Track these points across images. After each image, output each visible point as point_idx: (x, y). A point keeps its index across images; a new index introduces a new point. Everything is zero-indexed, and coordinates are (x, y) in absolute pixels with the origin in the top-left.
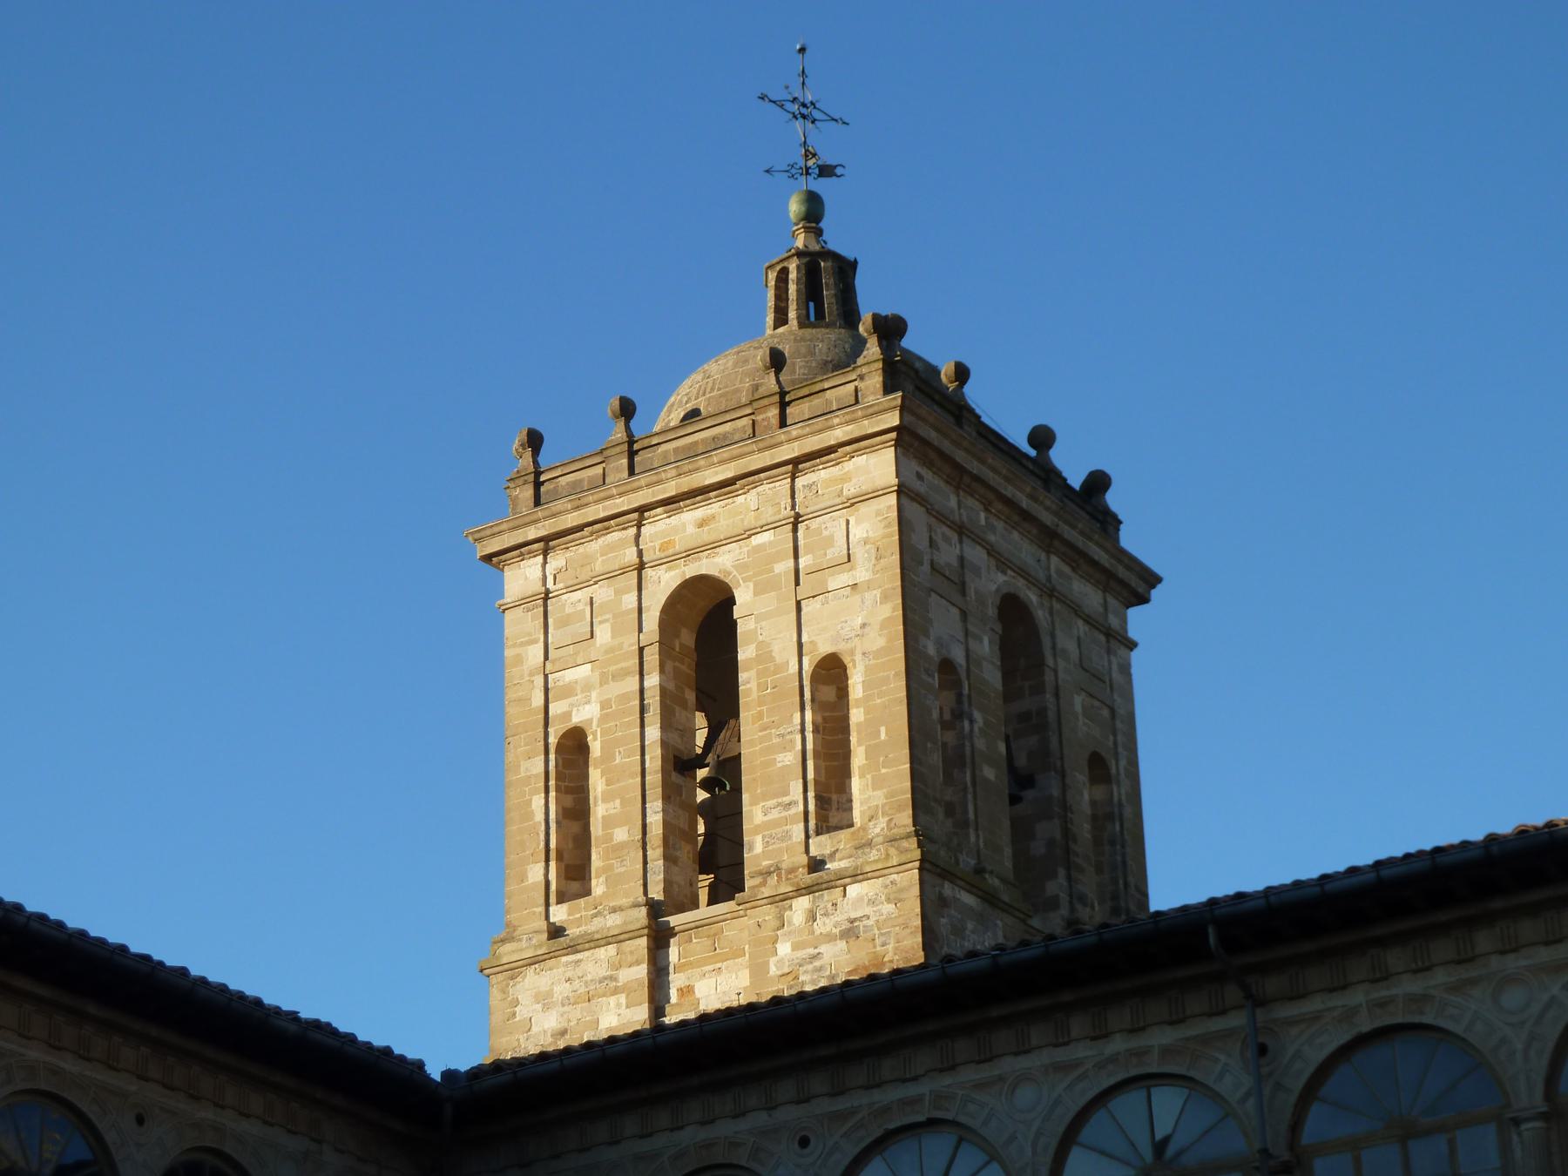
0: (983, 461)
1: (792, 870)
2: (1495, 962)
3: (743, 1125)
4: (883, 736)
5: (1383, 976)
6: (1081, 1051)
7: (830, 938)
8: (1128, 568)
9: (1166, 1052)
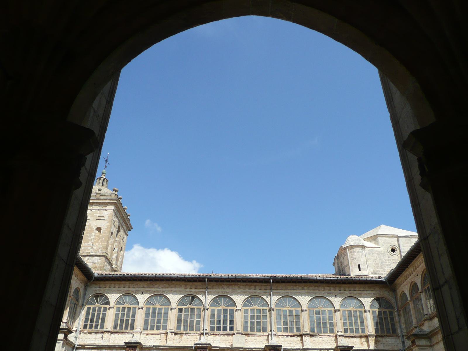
0: (122, 209)
1: (87, 252)
3: (134, 289)
4: (104, 239)
6: (183, 289)
7: (90, 262)
8: (130, 226)
9: (194, 292)
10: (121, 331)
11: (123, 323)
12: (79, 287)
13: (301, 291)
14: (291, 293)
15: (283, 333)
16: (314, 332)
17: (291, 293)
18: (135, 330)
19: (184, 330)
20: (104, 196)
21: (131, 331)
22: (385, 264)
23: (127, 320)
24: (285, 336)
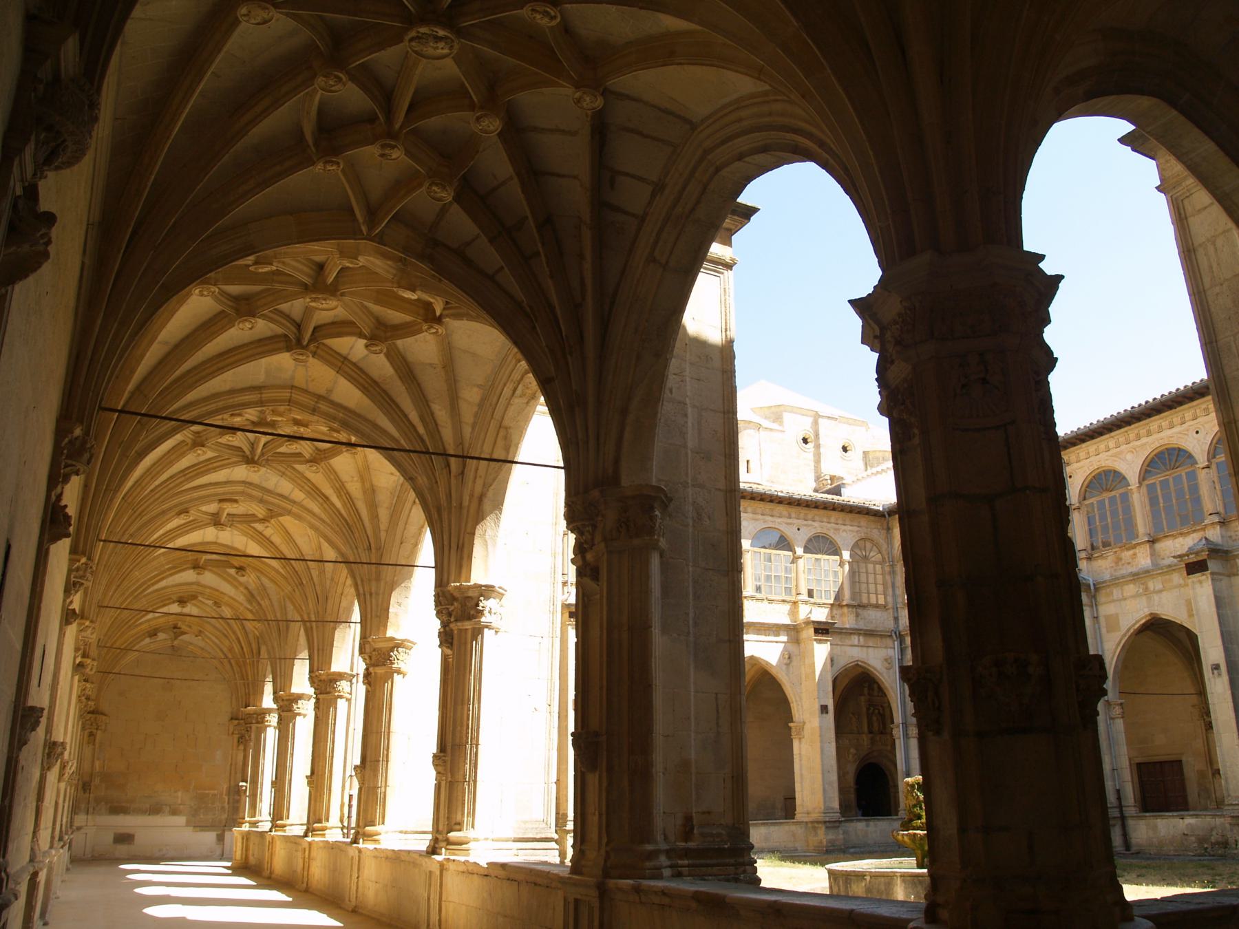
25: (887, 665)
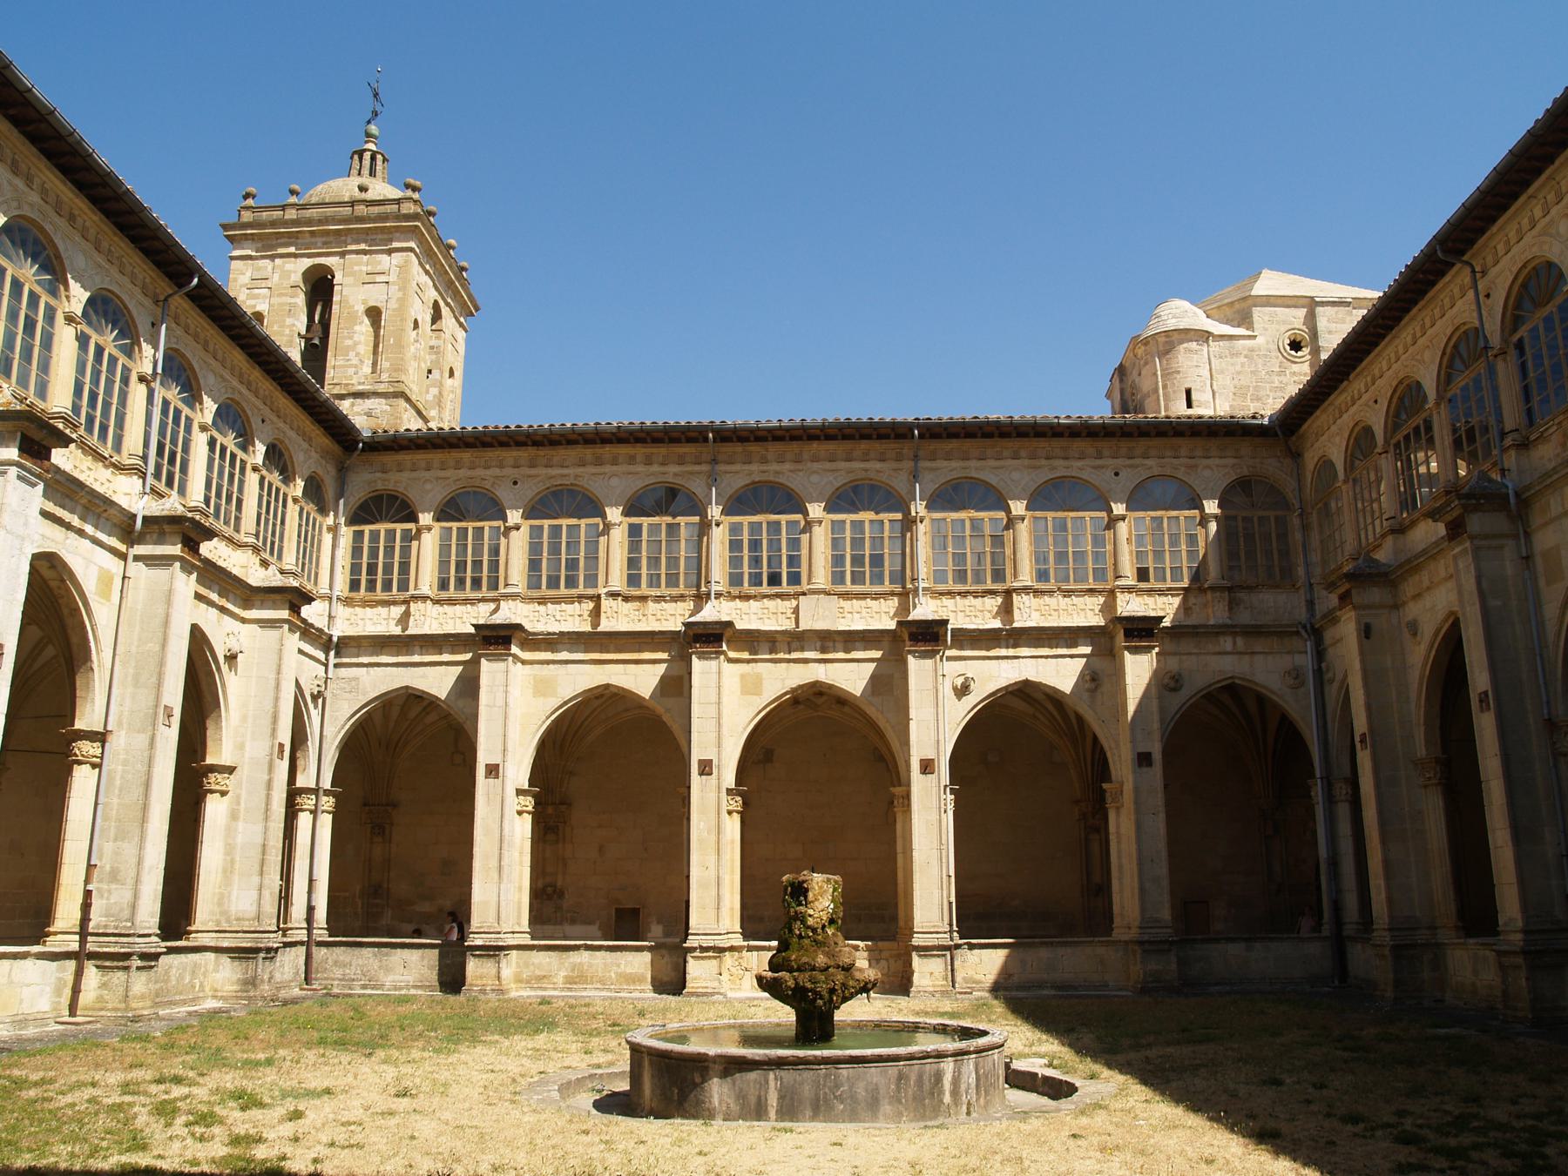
2: (809, 464)
3: (488, 472)
5: (764, 460)
9: (676, 475)
10: (461, 595)
11: (465, 572)
12: (320, 472)
13: (1010, 462)
14: (976, 469)
15: (951, 585)
16: (1047, 580)
17: (976, 469)
18: (503, 591)
19: (650, 585)
20: (377, 208)
21: (492, 594)
22: (1268, 385)
23: (477, 564)
24: (959, 594)
25: (1292, 682)
